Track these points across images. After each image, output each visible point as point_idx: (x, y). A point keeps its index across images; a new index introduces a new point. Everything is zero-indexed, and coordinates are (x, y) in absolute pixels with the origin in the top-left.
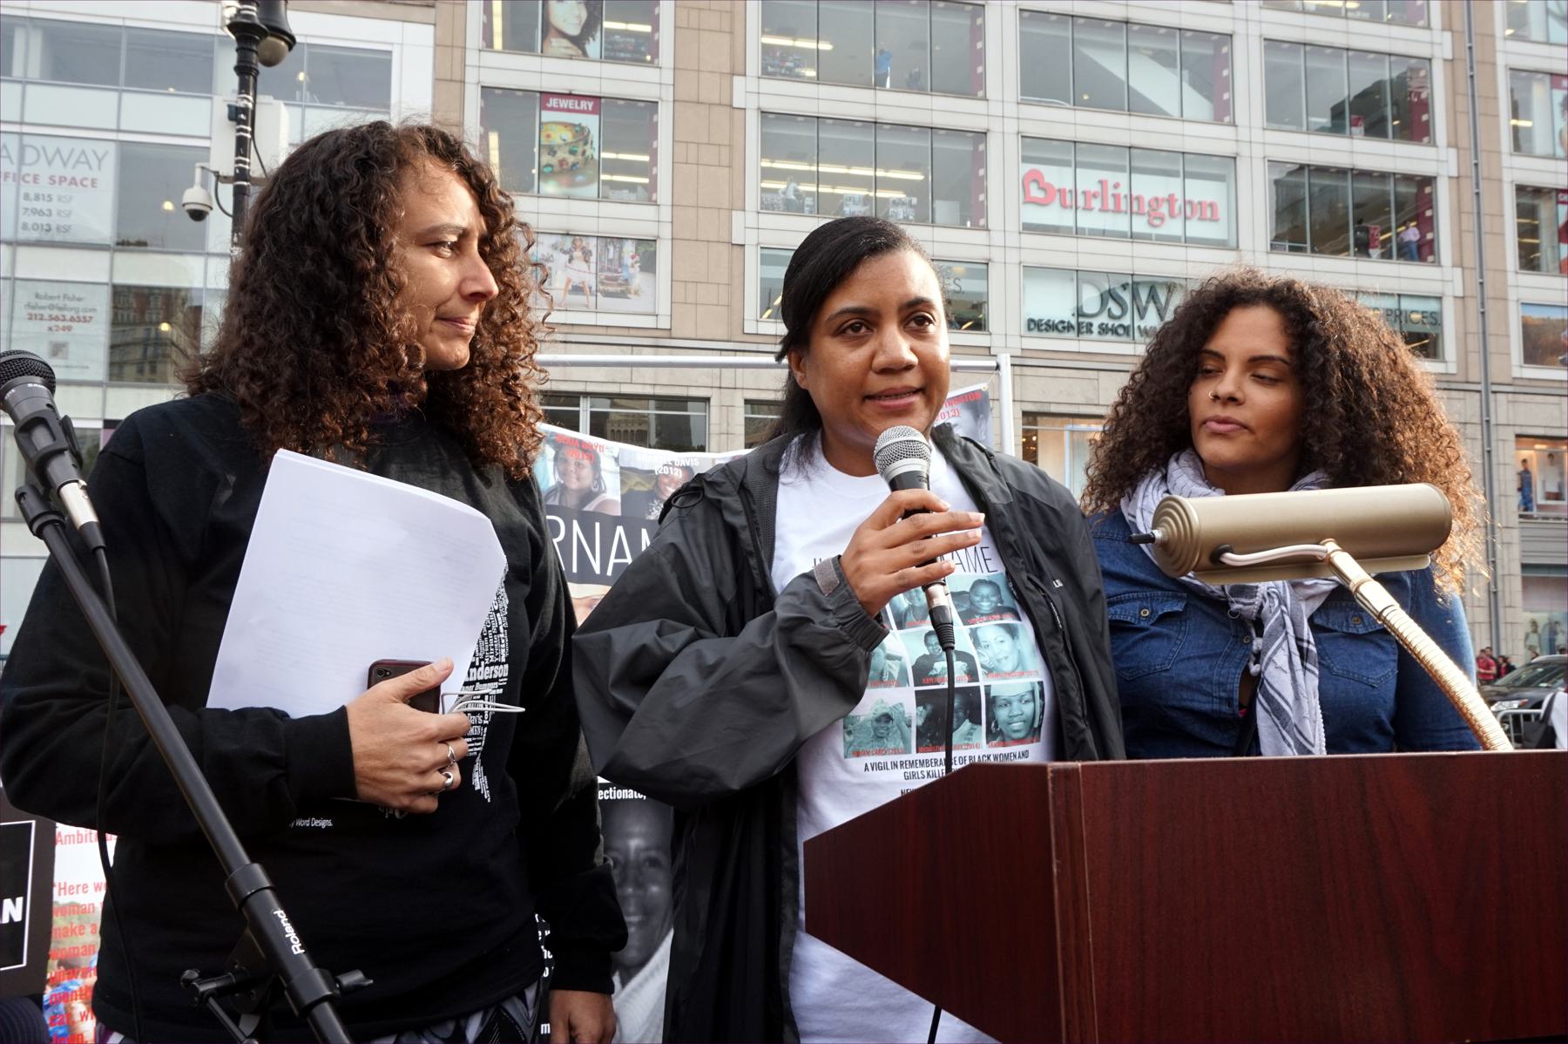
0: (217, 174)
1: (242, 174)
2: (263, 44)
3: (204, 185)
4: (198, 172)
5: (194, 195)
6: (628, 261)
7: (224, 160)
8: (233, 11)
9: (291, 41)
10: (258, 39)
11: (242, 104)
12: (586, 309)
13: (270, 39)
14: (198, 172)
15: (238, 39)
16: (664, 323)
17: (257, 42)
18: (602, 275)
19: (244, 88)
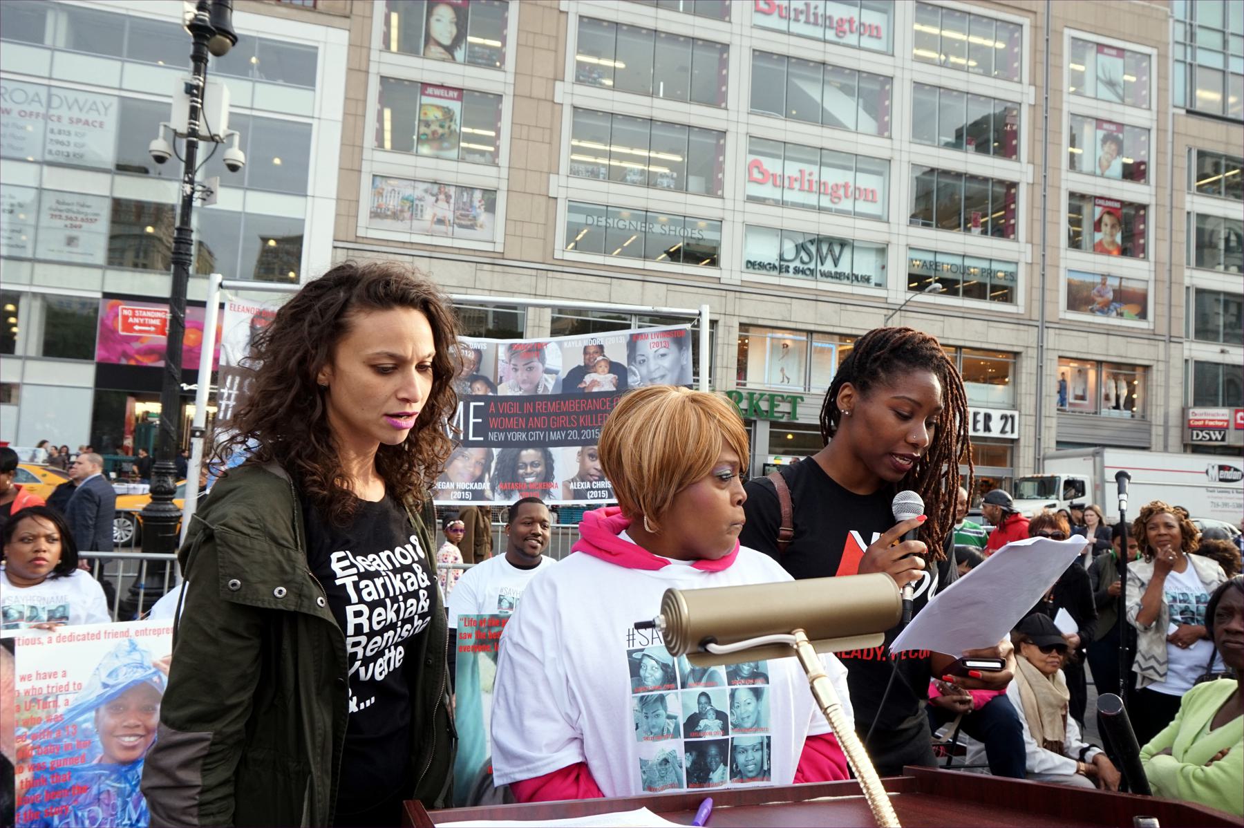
0: (175, 131)
1: (193, 133)
2: (213, 40)
3: (165, 139)
4: (162, 129)
5: (159, 145)
6: (476, 204)
7: (180, 121)
8: (190, 16)
9: (234, 39)
10: (209, 37)
11: (195, 82)
12: (446, 235)
13: (219, 37)
14: (162, 129)
15: (195, 36)
16: (499, 248)
17: (208, 39)
18: (458, 213)
19: (197, 71)
